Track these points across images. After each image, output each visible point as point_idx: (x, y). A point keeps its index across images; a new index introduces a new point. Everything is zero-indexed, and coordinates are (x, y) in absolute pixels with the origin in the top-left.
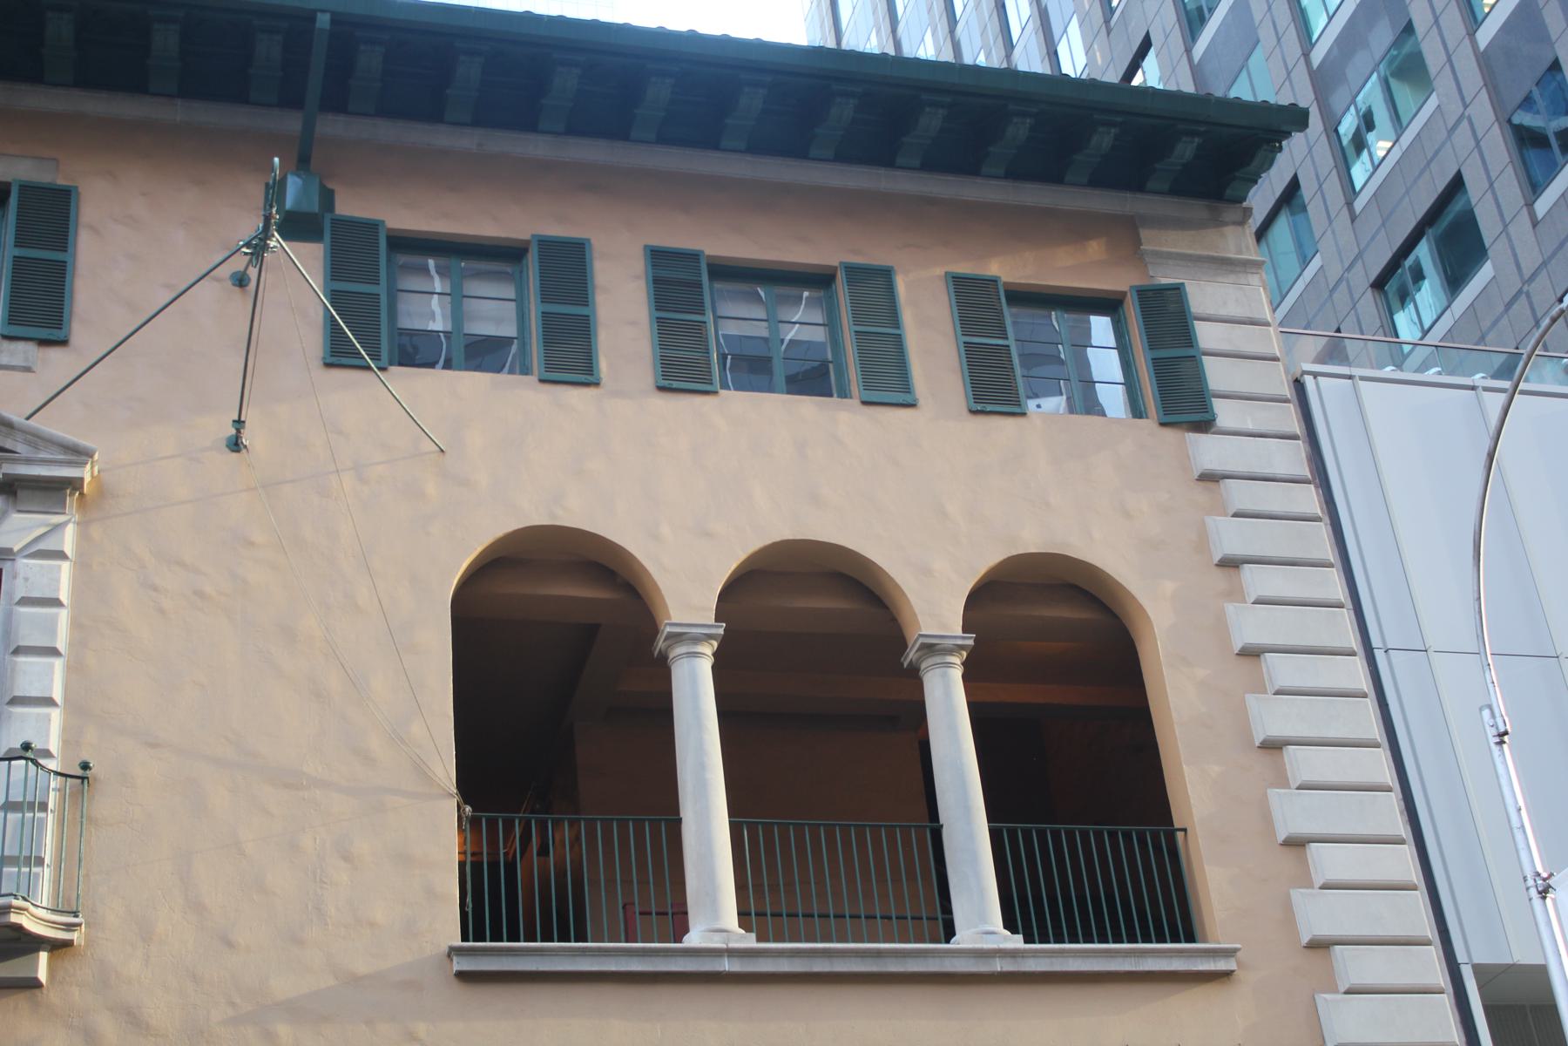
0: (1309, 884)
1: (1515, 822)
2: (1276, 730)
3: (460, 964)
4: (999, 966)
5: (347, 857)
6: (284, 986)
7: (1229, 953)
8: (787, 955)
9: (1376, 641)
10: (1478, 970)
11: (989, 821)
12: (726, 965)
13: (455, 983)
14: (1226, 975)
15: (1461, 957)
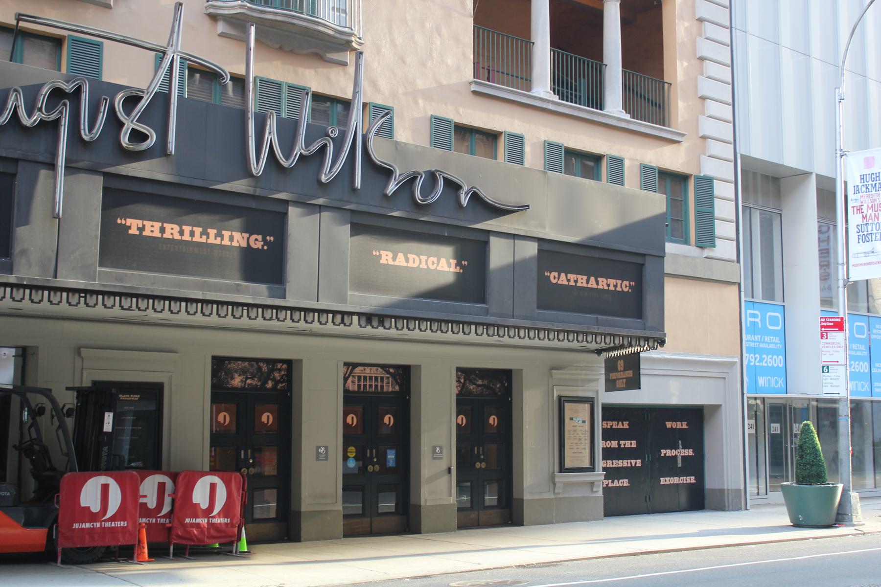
0: (704, 114)
1: (838, 130)
2: (705, 54)
3: (474, 88)
4: (623, 125)
5: (440, 35)
6: (421, 84)
7: (683, 135)
8: (568, 106)
9: (733, 26)
10: (742, 156)
11: (623, 67)
12: (551, 107)
13: (471, 95)
14: (679, 142)
15: (738, 151)
